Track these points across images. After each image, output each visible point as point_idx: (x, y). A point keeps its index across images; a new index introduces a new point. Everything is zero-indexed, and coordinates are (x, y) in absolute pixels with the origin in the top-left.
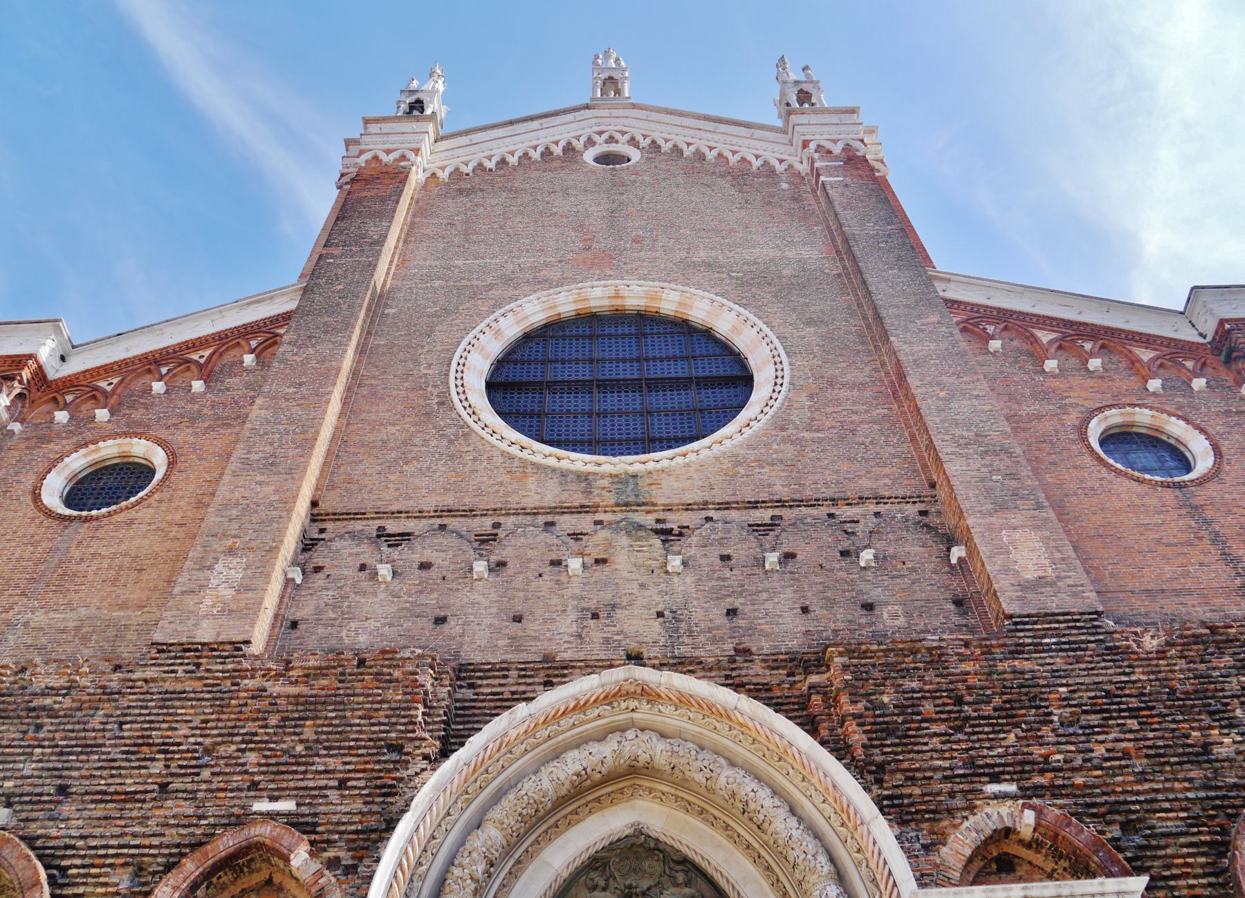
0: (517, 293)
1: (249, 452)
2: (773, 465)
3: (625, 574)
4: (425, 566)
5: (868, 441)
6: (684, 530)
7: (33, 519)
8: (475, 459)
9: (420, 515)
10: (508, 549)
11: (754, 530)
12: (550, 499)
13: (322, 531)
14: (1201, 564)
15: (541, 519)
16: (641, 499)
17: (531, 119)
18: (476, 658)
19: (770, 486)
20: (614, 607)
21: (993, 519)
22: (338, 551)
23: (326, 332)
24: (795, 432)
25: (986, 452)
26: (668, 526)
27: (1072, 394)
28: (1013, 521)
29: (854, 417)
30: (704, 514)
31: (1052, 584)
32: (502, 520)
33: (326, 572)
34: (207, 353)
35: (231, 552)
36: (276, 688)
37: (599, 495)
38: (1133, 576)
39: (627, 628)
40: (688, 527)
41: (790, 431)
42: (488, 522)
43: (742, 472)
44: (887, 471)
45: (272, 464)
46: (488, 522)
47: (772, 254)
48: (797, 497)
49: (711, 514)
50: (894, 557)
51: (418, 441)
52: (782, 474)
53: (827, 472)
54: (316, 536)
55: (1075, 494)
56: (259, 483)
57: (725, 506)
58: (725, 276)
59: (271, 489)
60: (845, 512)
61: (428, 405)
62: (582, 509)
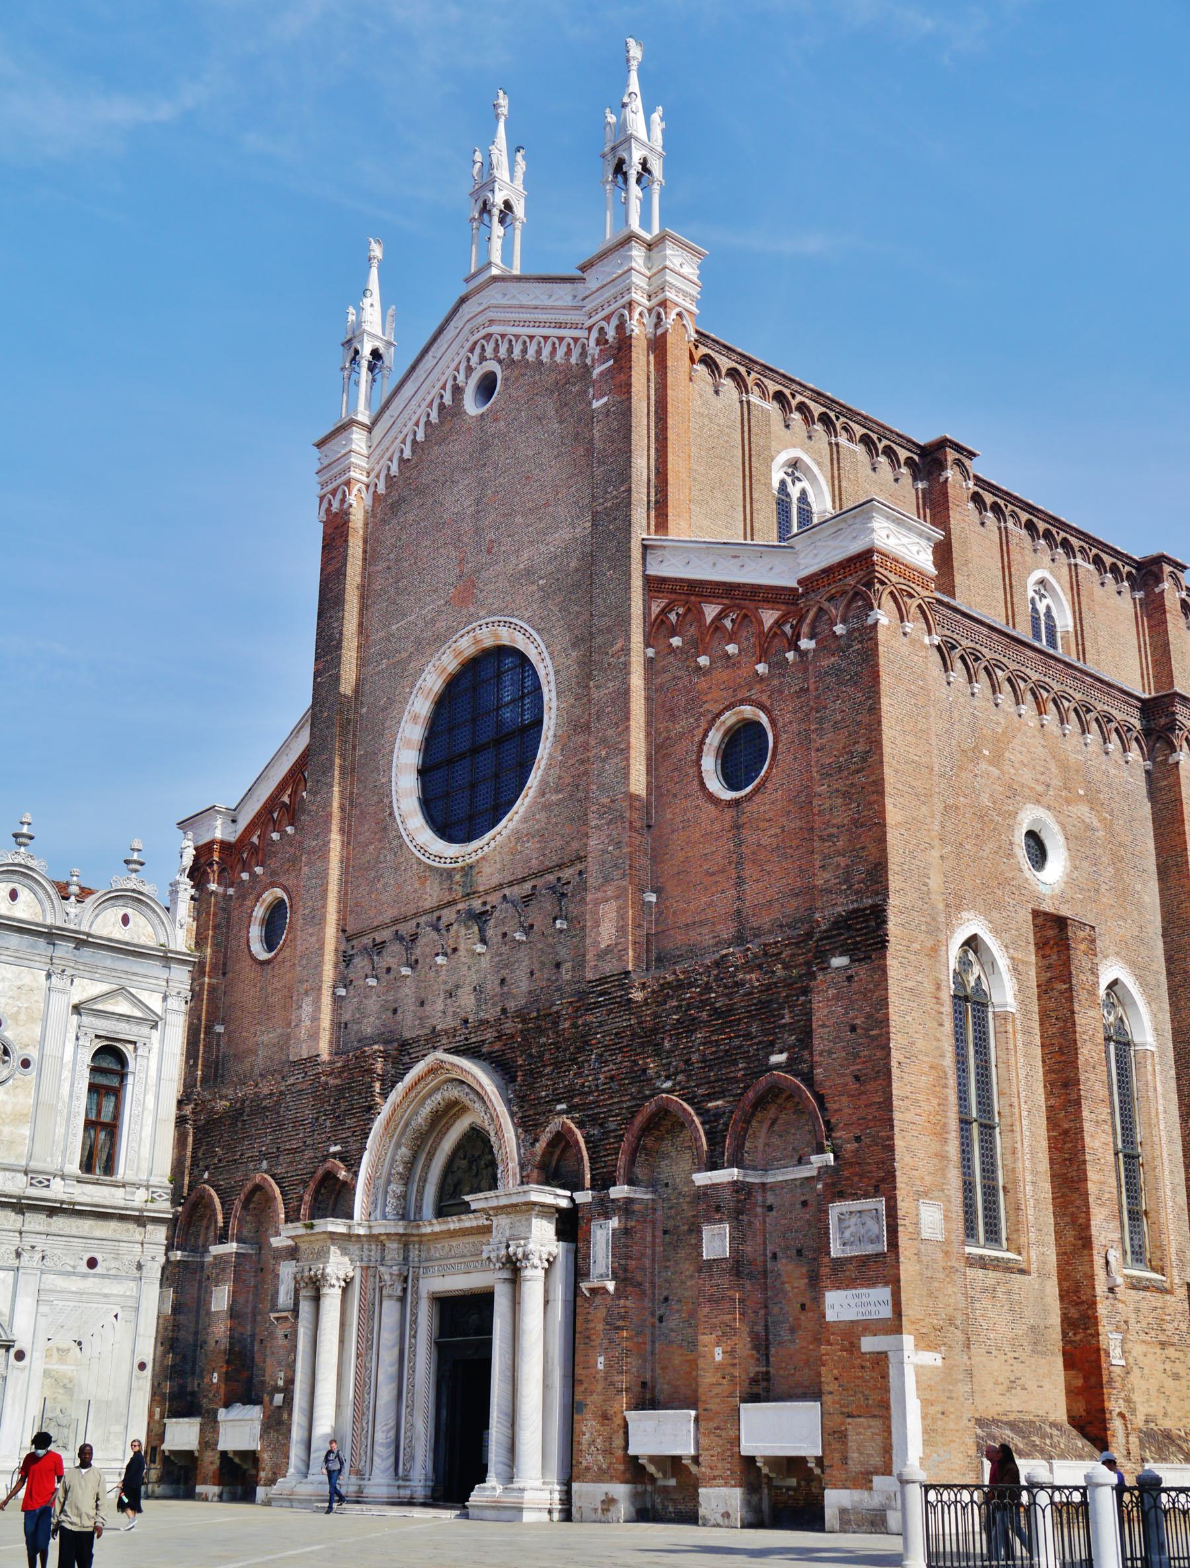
2: (533, 837)
3: (463, 959)
4: (389, 970)
14: (723, 891)
17: (426, 351)
18: (407, 1035)
20: (458, 986)
21: (600, 895)
23: (324, 773)
26: (488, 907)
27: (710, 696)
31: (611, 951)
33: (354, 983)
34: (289, 792)
35: (306, 993)
36: (333, 1082)
38: (684, 911)
39: (463, 1003)
41: (547, 796)
46: (414, 922)
49: (507, 891)
50: (576, 917)
51: (382, 858)
57: (511, 884)
62: (449, 904)
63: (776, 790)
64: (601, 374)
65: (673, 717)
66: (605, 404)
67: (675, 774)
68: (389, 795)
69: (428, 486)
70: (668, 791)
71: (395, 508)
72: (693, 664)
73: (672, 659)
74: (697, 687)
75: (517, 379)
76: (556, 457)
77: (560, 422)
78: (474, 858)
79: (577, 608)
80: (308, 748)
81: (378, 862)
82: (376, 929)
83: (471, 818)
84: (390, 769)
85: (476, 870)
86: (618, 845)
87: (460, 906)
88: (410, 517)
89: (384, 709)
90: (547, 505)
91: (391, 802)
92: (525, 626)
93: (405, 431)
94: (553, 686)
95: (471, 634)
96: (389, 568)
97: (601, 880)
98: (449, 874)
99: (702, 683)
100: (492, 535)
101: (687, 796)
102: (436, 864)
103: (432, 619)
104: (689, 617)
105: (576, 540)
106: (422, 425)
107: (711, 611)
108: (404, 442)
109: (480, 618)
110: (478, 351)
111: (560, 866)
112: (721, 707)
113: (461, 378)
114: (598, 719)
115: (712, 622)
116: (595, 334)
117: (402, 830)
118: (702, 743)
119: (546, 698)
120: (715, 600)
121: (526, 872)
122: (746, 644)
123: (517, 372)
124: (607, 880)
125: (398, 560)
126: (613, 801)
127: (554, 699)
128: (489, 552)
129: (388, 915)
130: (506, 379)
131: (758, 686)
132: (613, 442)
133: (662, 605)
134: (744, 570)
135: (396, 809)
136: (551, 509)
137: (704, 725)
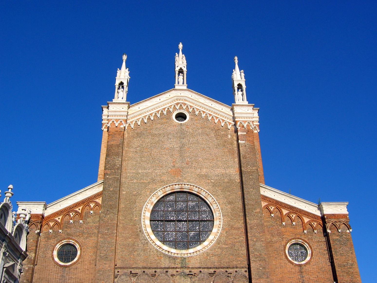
0: (156, 186)
1: (101, 253)
2: (215, 256)
5: (237, 249)
6: (195, 274)
7: (55, 266)
8: (149, 251)
9: (139, 268)
10: (159, 280)
11: (210, 275)
12: (167, 266)
13: (118, 272)
15: (165, 270)
16: (186, 266)
19: (214, 263)
21: (257, 281)
22: (123, 279)
24: (221, 245)
25: (260, 260)
27: (286, 234)
28: (261, 281)
29: (235, 240)
30: (200, 270)
32: (156, 270)
34: (81, 208)
37: (177, 264)
40: (196, 274)
41: (220, 245)
42: (154, 270)
43: (209, 258)
44: (240, 259)
45: (107, 258)
46: (154, 270)
48: (219, 266)
49: (201, 270)
51: (136, 244)
52: (217, 259)
53: (227, 259)
54: (117, 274)
55: (278, 268)
56: (105, 264)
57: (204, 268)
58: (210, 181)
59: (107, 266)
60: (230, 270)
61: (137, 231)
63: (314, 265)
66: (244, 143)
70: (273, 256)
71: (139, 135)
81: (133, 245)
82: (133, 268)
85: (187, 261)
86: (264, 268)
87: (177, 270)
88: (147, 140)
90: (213, 160)
95: (180, 185)
97: (257, 277)
98: (175, 258)
99: (283, 229)
101: (281, 259)
107: (285, 212)
109: (183, 182)
110: (179, 106)
111: (227, 268)
112: (291, 238)
113: (171, 110)
120: (286, 209)
121: (213, 266)
124: (260, 277)
128: (187, 164)
129: (140, 265)
130: (191, 119)
131: (304, 236)
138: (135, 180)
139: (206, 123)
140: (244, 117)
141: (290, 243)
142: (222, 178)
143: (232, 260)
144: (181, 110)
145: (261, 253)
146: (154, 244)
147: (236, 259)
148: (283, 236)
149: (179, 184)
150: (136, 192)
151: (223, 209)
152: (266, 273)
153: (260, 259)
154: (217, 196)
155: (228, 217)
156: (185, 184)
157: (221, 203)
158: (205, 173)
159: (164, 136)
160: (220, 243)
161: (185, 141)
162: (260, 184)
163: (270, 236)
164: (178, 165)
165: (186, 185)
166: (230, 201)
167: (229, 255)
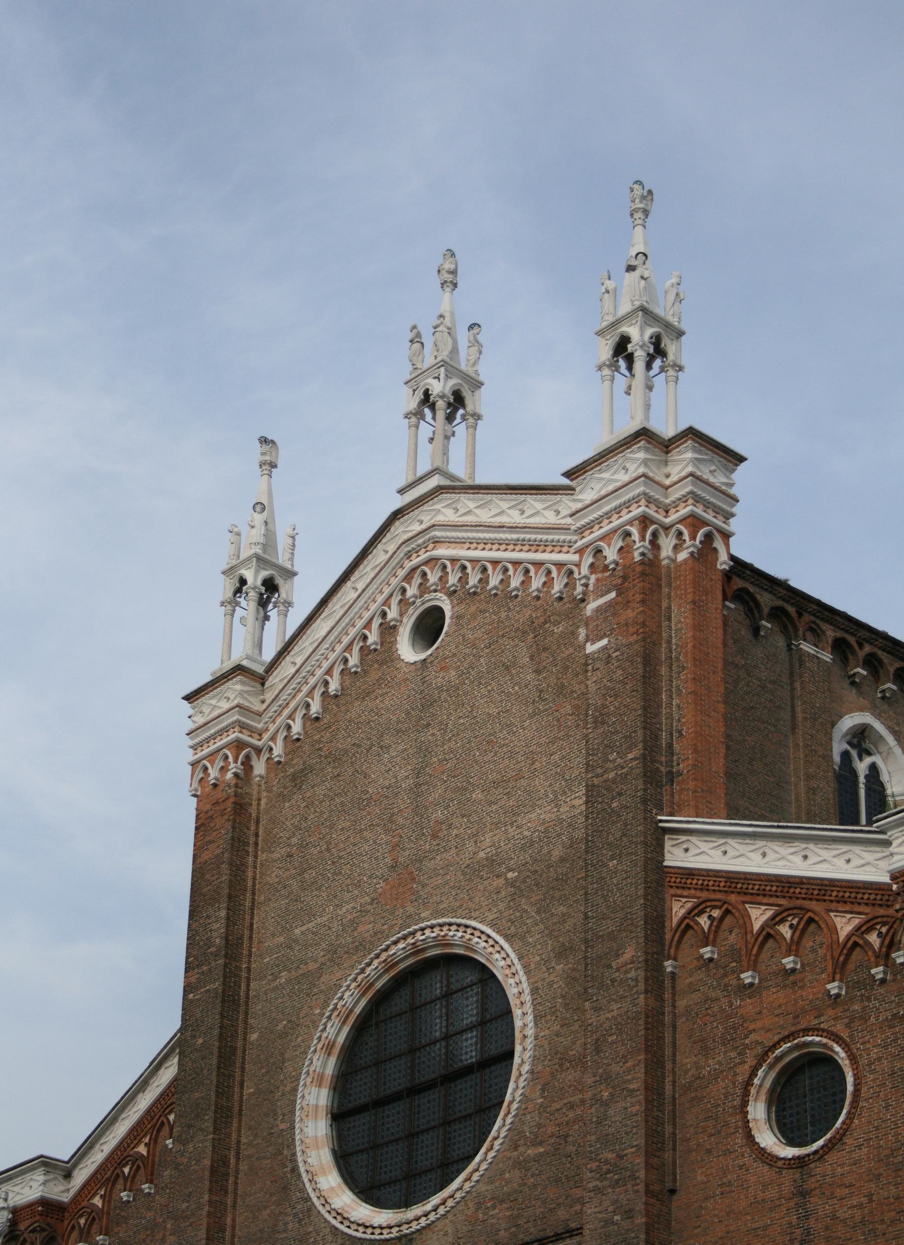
0: (339, 974)
2: (502, 1202)
23: (197, 1116)
27: (759, 1024)
41: (521, 1149)
47: (548, 817)
51: (281, 1226)
64: (598, 610)
65: (706, 1051)
66: (604, 648)
67: (710, 1123)
68: (291, 1145)
69: (346, 752)
70: (698, 1145)
72: (734, 982)
73: (703, 975)
74: (741, 1011)
75: (474, 617)
76: (531, 716)
77: (538, 672)
78: (415, 1226)
79: (562, 909)
80: (175, 1080)
83: (408, 1177)
84: (293, 1112)
88: (321, 791)
89: (284, 1035)
90: (519, 777)
91: (294, 1154)
92: (489, 931)
93: (312, 681)
94: (528, 1007)
95: (410, 940)
96: (290, 855)
99: (749, 1006)
100: (439, 815)
101: (727, 1153)
102: (359, 1235)
103: (352, 921)
104: (728, 920)
105: (561, 821)
106: (336, 672)
107: (759, 916)
108: (310, 693)
110: (417, 580)
112: (776, 1038)
113: (392, 614)
114: (598, 1051)
115: (762, 928)
116: (588, 560)
117: (310, 1190)
118: (749, 1083)
119: (518, 1023)
120: (765, 900)
122: (811, 957)
123: (473, 609)
125: (303, 846)
126: (621, 1157)
127: (531, 1025)
128: (435, 836)
130: (457, 617)
132: (616, 696)
133: (689, 905)
134: (810, 861)
135: (301, 1164)
136: (524, 782)
137: (751, 1061)
138: (285, 973)
139: (503, 615)
140: (599, 521)
141: (771, 1067)
142: (545, 851)
143: (554, 1206)
144: (427, 597)
145: (626, 1149)
146: (327, 1207)
147: (567, 1197)
148: (746, 1037)
149: (405, 938)
150: (285, 1022)
151: (537, 988)
152: (633, 1235)
153: (616, 1177)
154: (522, 938)
155: (553, 1018)
156: (423, 929)
157: (533, 966)
158: (489, 850)
159: (372, 745)
160: (519, 1143)
161: (433, 735)
162: (661, 821)
163: (695, 1056)
164: (408, 852)
165: (428, 932)
166: (563, 945)
167: (545, 1188)
